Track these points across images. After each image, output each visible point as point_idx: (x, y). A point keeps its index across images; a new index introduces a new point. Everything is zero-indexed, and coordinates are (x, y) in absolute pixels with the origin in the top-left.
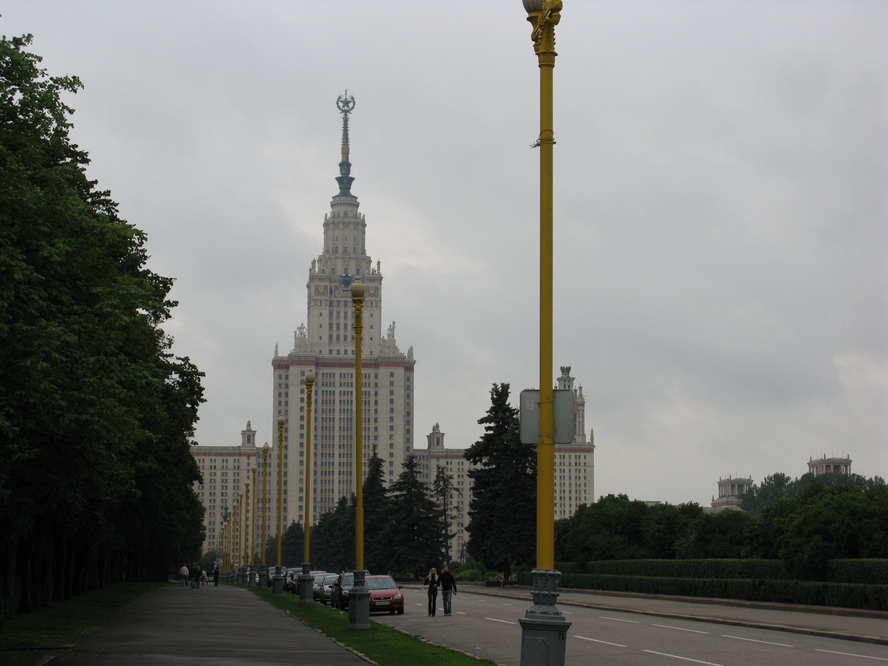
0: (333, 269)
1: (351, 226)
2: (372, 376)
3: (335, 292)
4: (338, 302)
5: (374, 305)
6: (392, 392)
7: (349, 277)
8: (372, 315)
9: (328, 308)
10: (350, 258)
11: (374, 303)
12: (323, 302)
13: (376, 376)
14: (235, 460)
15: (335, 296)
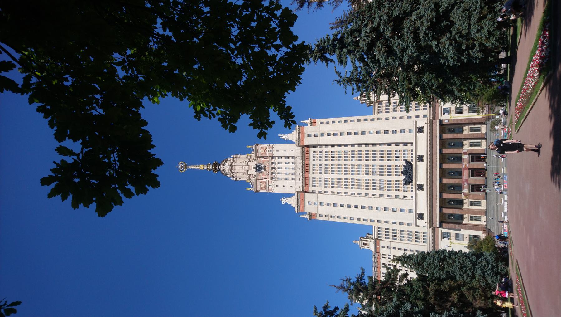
0: (255, 176)
1: (233, 164)
2: (314, 149)
3: (266, 176)
4: (272, 173)
5: (272, 150)
6: (322, 135)
7: (257, 166)
8: (277, 151)
9: (273, 181)
10: (248, 166)
11: (270, 150)
12: (270, 184)
13: (314, 146)
14: (383, 257)
15: (268, 175)
